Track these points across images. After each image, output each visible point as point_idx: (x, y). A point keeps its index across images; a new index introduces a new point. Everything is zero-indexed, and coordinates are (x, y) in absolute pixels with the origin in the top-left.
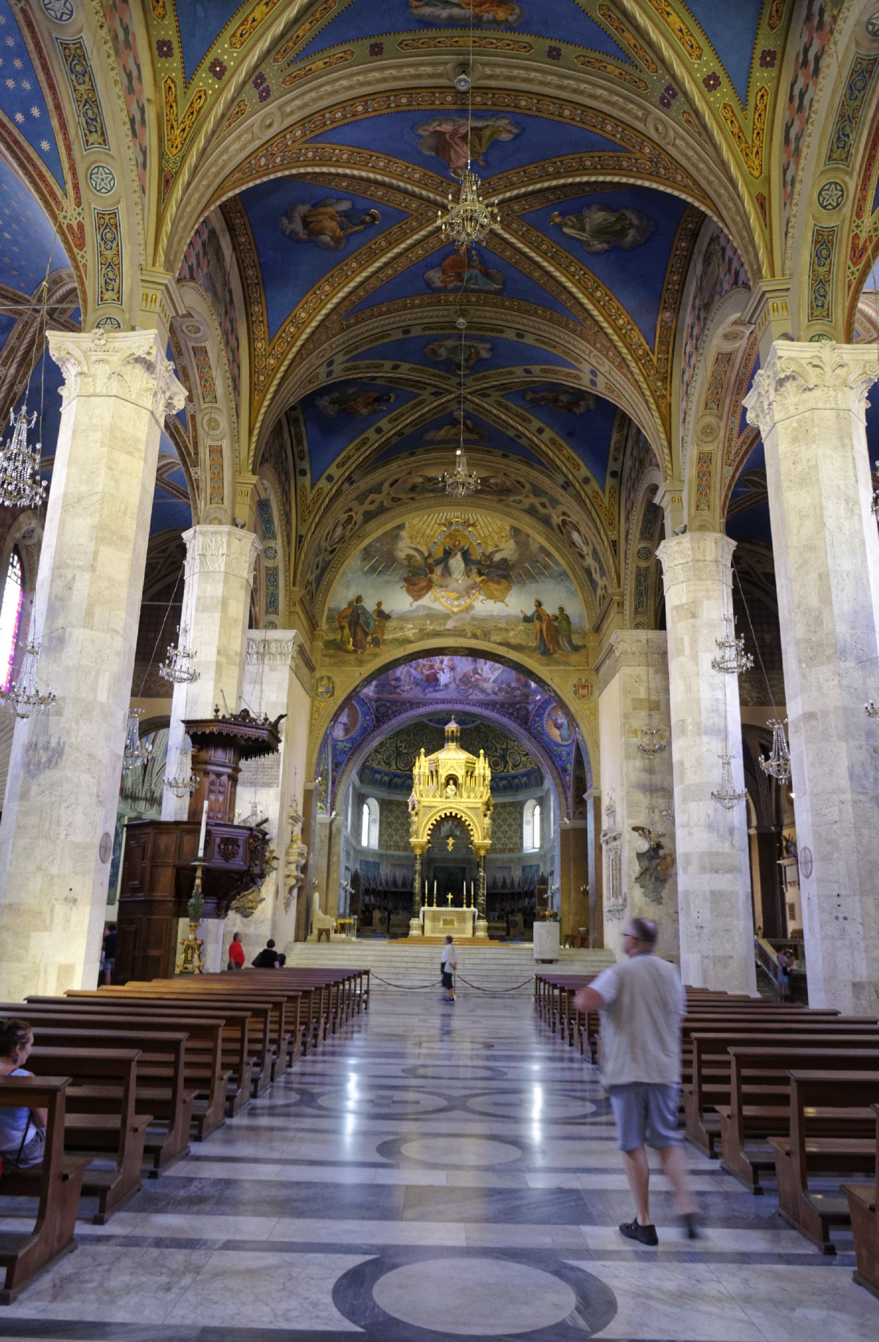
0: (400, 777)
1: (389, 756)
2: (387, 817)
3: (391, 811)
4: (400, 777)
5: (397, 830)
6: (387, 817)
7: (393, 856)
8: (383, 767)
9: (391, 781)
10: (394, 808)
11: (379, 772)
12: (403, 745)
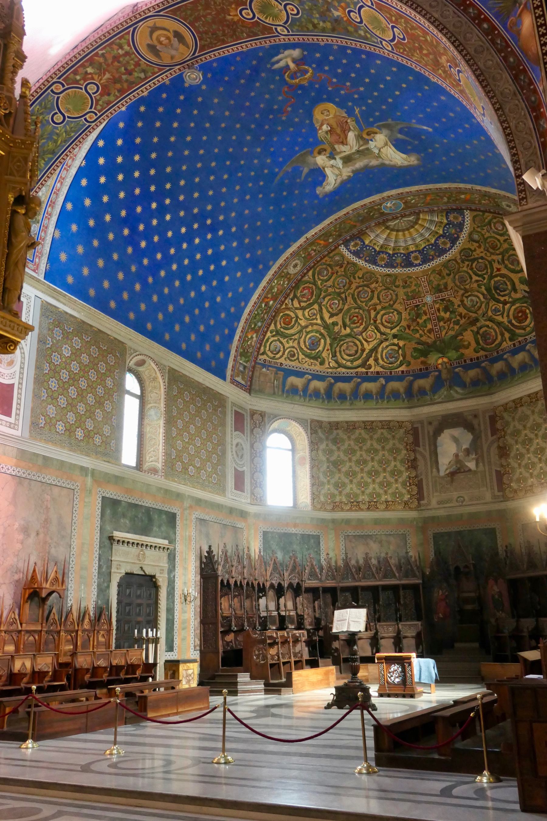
0: (346, 379)
1: (314, 345)
2: (331, 452)
3: (335, 441)
4: (346, 379)
5: (351, 474)
6: (331, 452)
7: (348, 522)
8: (307, 365)
9: (331, 386)
10: (341, 434)
11: (299, 374)
12: (338, 319)
